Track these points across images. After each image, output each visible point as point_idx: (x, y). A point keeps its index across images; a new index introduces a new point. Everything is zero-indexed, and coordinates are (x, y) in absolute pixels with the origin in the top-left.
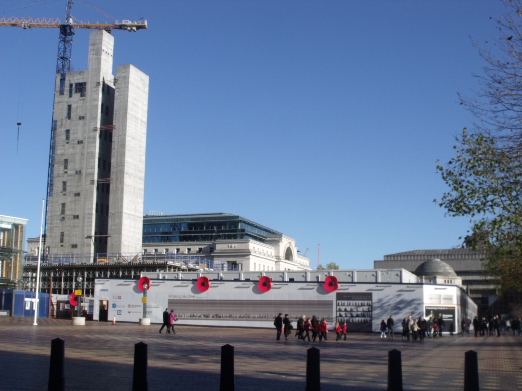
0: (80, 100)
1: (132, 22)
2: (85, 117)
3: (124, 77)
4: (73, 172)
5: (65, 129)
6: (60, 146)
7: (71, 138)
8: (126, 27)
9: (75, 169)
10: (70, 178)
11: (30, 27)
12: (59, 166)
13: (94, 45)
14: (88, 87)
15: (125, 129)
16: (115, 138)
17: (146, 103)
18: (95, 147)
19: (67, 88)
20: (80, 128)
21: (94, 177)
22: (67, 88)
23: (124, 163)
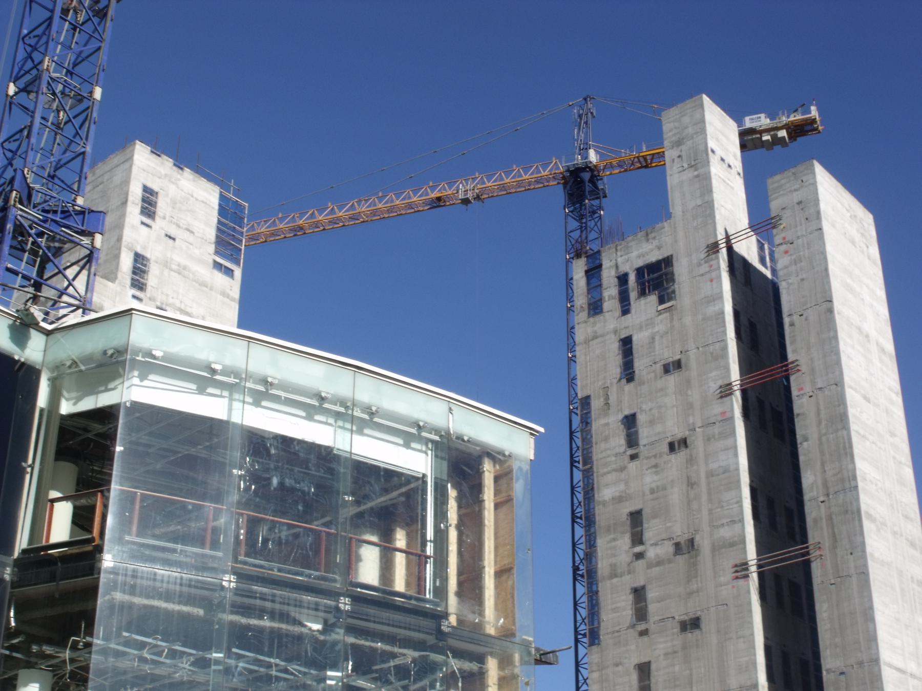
0: (659, 313)
1: (771, 120)
2: (683, 362)
3: (800, 203)
4: (668, 549)
5: (620, 417)
6: (609, 473)
7: (643, 441)
8: (758, 136)
9: (670, 539)
10: (656, 571)
11: (478, 198)
12: (614, 540)
13: (679, 143)
14: (681, 269)
15: (838, 363)
16: (802, 404)
17: (881, 293)
18: (735, 447)
19: (610, 291)
20: (670, 400)
21: (744, 550)
22: (610, 291)
23: (855, 478)
